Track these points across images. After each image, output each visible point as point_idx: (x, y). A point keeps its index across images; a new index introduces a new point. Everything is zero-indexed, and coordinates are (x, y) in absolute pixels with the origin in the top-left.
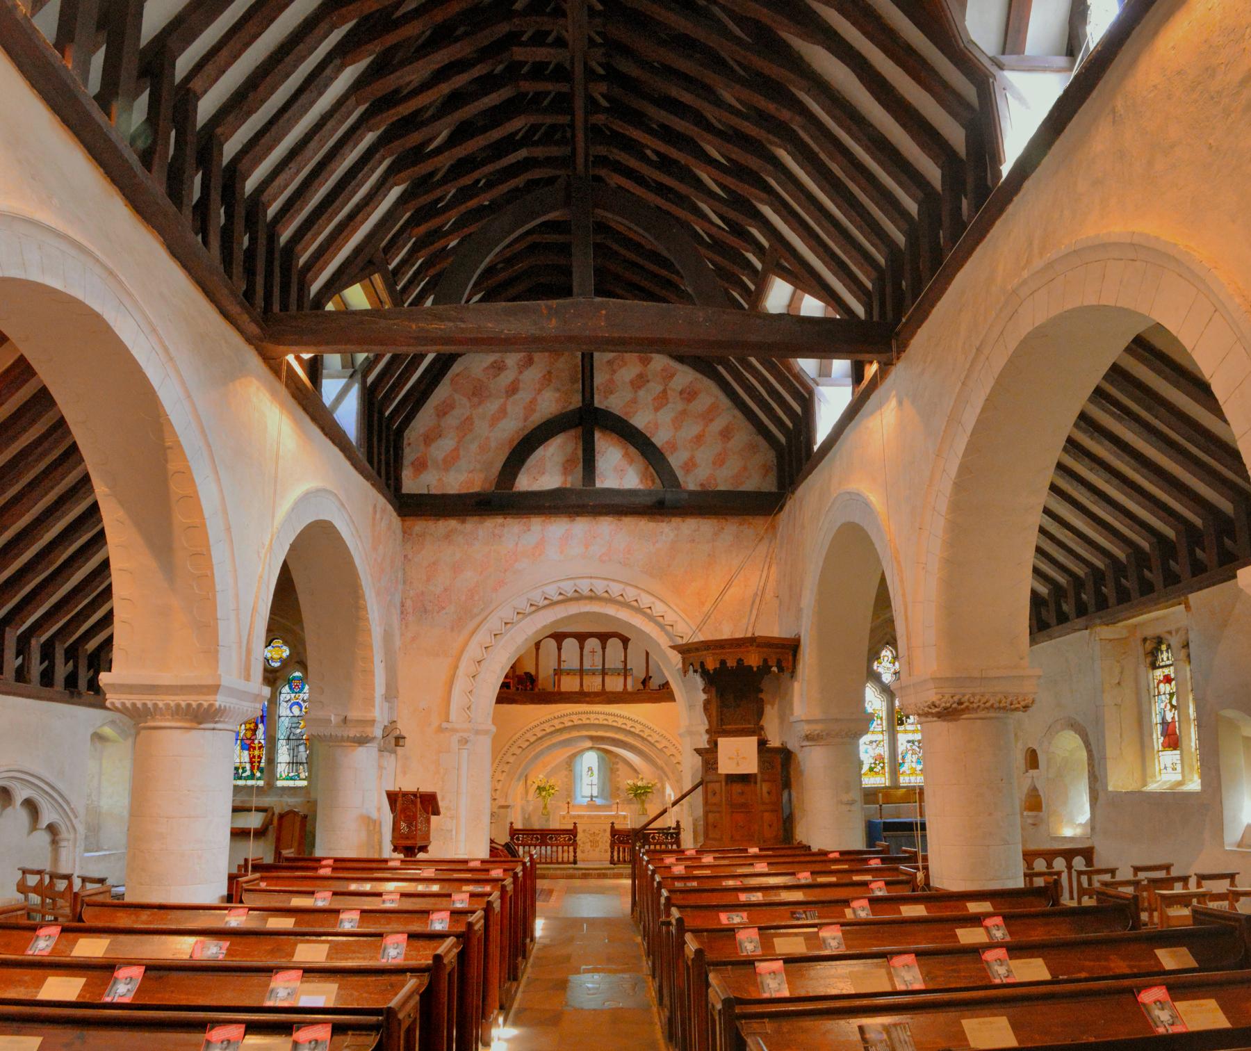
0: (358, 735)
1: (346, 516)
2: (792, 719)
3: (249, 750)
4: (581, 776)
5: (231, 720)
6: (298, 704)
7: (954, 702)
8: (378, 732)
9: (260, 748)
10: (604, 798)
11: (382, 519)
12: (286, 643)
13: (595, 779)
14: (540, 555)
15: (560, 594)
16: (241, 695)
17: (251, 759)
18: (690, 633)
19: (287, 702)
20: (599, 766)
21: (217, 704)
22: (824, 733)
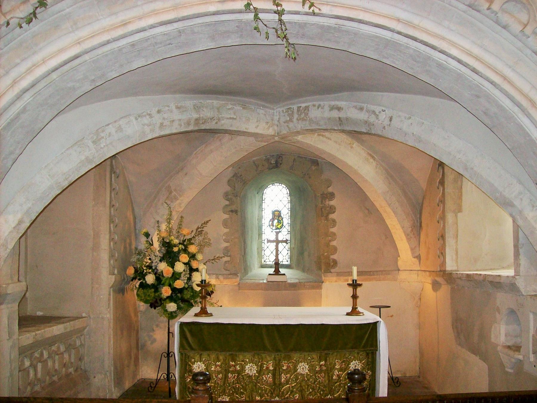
4: (260, 228)
20: (293, 210)
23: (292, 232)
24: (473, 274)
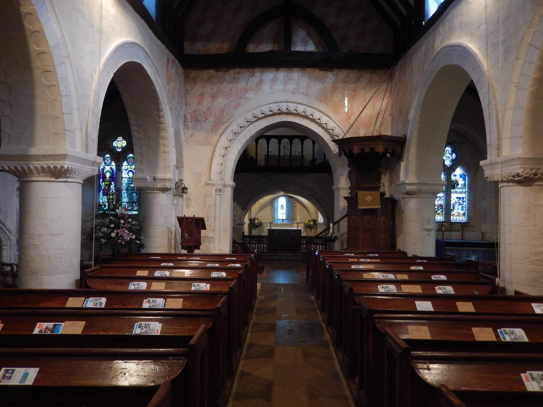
0: (162, 187)
1: (150, 61)
2: (398, 183)
3: (107, 196)
5: (77, 177)
6: (132, 171)
7: (532, 174)
8: (173, 186)
9: (112, 195)
10: (289, 221)
11: (172, 67)
12: (124, 139)
13: (284, 211)
14: (259, 89)
15: (270, 111)
16: (84, 161)
17: (108, 200)
18: (340, 134)
19: (126, 170)
21: (66, 166)
22: (417, 191)
23: (286, 210)
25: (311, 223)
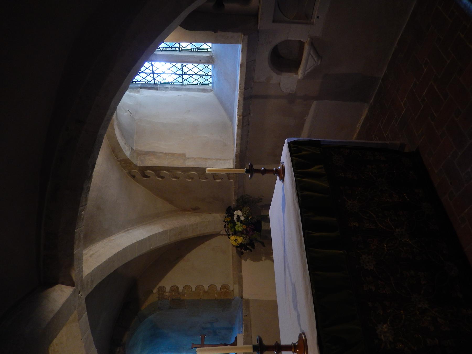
24: (238, 115)
25: (239, 217)
